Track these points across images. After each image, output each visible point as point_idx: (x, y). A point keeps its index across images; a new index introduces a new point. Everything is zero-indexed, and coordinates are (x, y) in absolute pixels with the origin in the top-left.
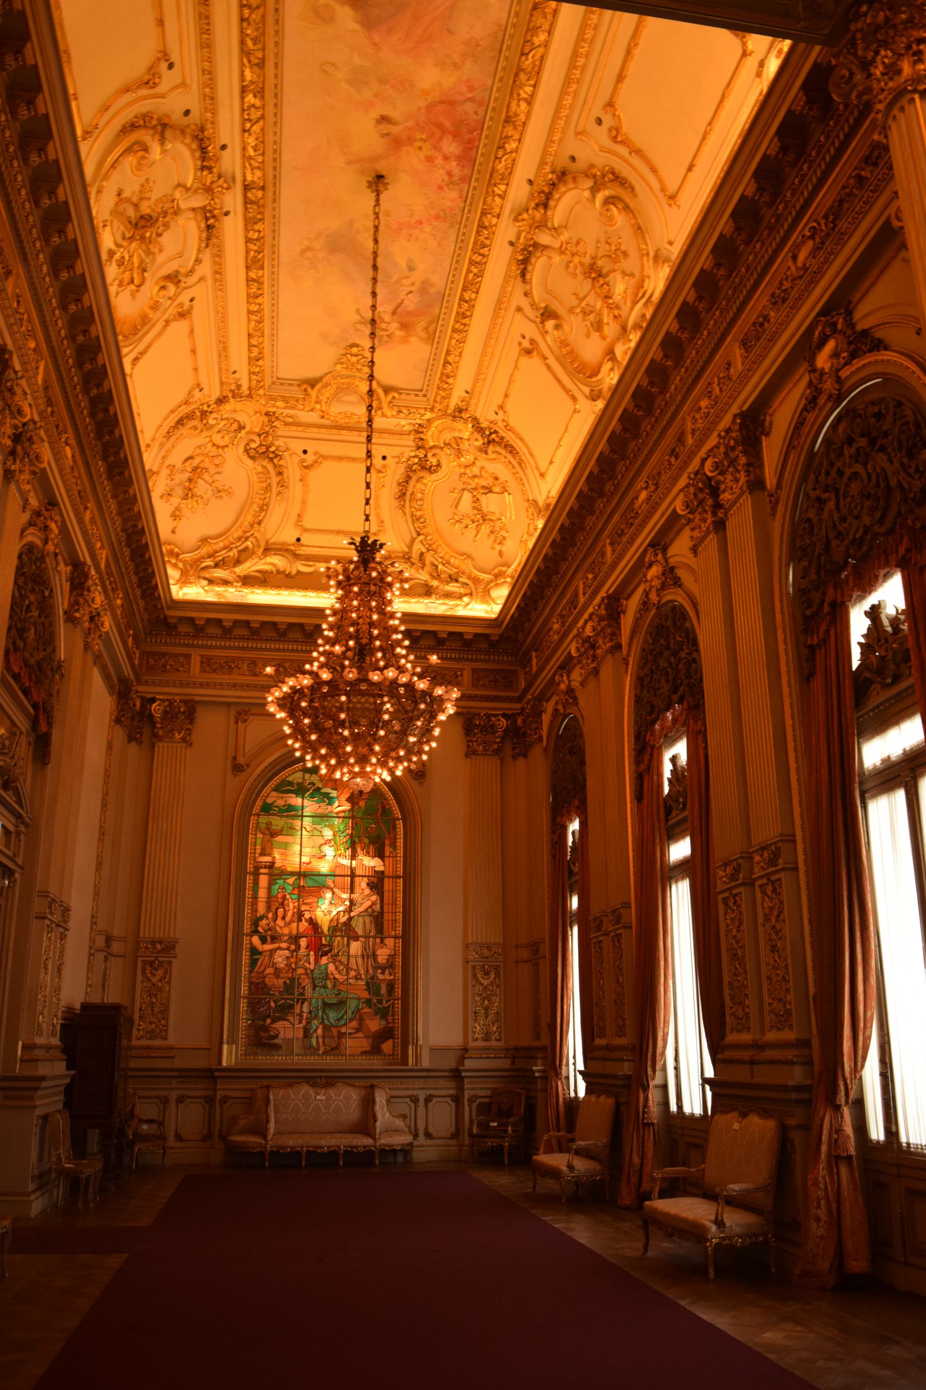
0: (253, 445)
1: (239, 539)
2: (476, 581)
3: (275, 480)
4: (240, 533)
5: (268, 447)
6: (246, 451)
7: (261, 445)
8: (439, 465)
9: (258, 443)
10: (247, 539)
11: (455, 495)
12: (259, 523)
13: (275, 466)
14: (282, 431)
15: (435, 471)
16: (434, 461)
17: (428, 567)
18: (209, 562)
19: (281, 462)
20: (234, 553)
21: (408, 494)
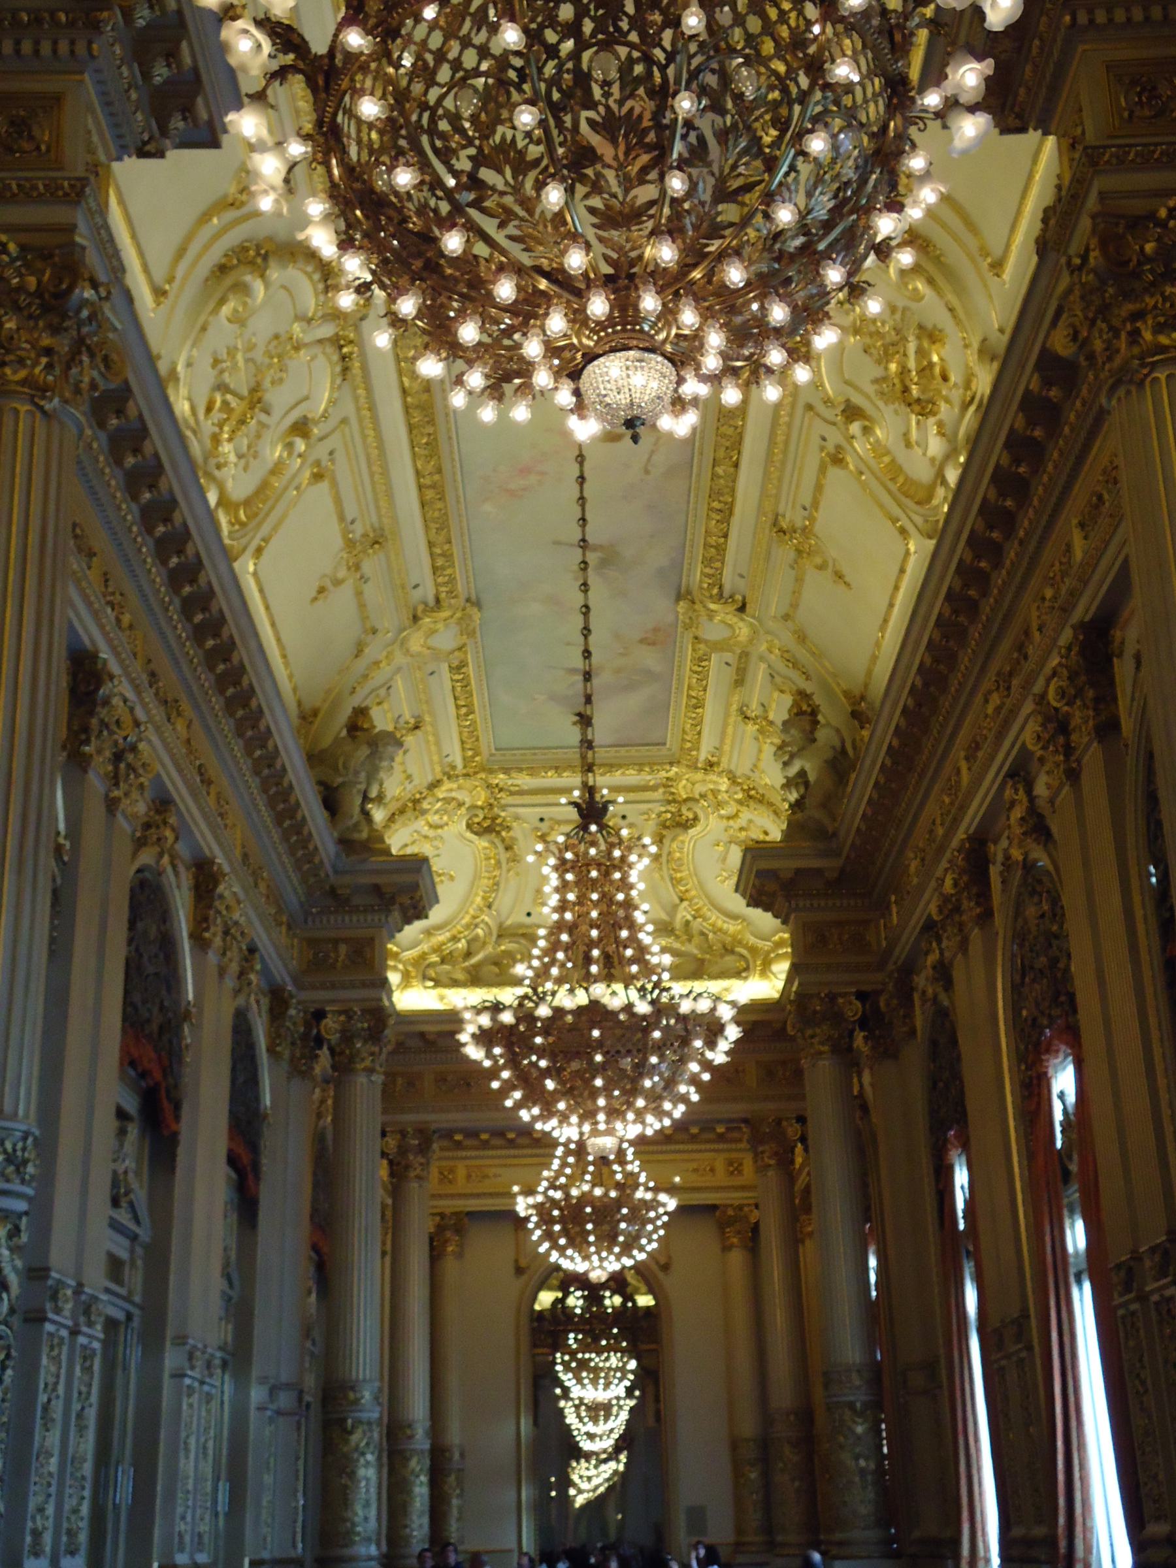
0: (476, 820)
1: (467, 927)
2: (753, 950)
3: (504, 856)
4: (467, 919)
5: (494, 819)
6: (469, 826)
7: (485, 818)
8: (696, 818)
9: (481, 816)
10: (476, 926)
11: (721, 848)
12: (489, 907)
13: (503, 840)
14: (506, 799)
15: (692, 826)
16: (691, 816)
17: (697, 940)
18: (434, 958)
19: (511, 833)
20: (462, 945)
21: (664, 859)
